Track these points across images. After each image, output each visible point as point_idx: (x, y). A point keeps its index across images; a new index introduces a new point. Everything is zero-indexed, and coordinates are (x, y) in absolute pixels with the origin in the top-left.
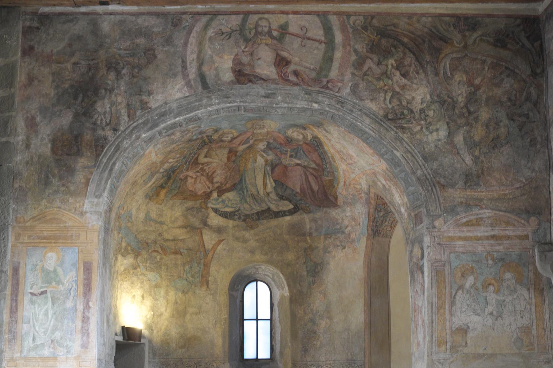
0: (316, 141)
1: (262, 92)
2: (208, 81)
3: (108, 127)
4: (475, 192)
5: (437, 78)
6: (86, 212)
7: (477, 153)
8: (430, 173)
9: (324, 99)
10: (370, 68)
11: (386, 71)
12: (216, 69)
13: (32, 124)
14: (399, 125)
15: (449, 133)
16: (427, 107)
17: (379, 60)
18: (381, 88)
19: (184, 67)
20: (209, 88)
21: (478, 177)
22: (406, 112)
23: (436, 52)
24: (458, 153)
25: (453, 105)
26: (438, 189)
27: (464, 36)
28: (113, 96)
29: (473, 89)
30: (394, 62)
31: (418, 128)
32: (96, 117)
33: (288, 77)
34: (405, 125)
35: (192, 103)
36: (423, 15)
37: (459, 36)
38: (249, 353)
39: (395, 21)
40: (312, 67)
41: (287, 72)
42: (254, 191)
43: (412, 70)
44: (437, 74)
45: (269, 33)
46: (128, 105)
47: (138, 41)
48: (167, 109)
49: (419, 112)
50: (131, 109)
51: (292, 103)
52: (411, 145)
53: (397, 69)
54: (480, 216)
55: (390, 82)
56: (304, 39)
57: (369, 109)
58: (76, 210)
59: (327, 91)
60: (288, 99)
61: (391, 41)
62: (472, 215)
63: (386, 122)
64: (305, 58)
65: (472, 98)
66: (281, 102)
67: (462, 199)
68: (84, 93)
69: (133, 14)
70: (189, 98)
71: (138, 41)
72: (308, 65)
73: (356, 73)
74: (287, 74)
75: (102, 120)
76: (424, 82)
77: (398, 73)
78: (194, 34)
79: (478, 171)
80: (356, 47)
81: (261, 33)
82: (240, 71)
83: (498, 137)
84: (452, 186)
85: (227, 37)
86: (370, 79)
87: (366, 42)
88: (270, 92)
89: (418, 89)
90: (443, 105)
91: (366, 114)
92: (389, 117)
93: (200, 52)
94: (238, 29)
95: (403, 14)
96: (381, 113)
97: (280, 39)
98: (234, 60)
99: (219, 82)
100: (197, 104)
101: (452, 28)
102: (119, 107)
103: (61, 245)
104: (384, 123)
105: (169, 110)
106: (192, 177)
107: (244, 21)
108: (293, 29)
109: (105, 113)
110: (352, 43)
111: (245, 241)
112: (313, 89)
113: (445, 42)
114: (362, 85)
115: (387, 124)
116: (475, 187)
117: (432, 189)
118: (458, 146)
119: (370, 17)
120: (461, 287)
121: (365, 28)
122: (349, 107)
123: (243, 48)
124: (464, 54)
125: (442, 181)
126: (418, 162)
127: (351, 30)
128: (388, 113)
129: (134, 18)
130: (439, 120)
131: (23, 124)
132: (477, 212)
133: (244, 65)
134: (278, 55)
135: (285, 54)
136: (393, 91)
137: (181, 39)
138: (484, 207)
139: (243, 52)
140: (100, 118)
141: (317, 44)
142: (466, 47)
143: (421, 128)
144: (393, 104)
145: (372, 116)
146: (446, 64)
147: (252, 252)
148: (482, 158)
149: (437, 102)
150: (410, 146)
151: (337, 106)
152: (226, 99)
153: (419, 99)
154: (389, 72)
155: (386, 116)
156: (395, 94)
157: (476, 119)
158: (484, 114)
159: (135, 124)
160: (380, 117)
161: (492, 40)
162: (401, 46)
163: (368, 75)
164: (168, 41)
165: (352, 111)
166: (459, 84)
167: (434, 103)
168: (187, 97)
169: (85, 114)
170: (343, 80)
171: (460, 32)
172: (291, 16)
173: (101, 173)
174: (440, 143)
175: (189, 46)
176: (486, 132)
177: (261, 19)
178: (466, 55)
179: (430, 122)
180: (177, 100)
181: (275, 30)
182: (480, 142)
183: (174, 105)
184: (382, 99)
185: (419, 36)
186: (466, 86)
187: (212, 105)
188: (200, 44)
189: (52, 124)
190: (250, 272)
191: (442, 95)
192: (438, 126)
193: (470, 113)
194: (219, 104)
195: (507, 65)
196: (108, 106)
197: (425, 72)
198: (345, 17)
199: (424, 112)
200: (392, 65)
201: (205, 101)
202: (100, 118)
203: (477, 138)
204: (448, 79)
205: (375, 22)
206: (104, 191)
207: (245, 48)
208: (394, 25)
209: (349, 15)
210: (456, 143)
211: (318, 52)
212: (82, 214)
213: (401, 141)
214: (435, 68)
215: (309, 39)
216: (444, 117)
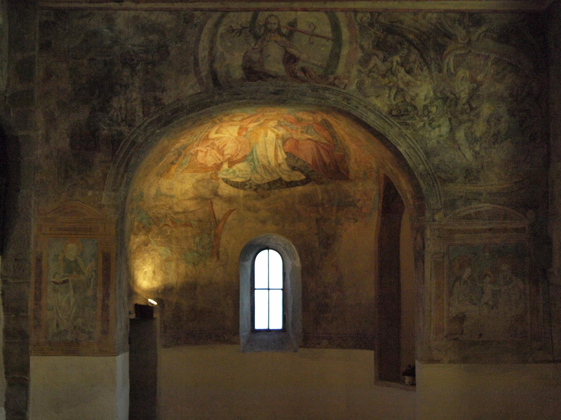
1: (271, 89)
2: (219, 78)
3: (124, 123)
4: (475, 186)
5: (441, 75)
6: (104, 206)
7: (477, 149)
8: (432, 168)
9: (331, 96)
10: (376, 65)
11: (391, 68)
12: (228, 65)
13: (51, 120)
14: (402, 121)
15: (451, 129)
16: (430, 103)
17: (385, 57)
18: (386, 85)
19: (196, 64)
20: (220, 85)
21: (478, 172)
22: (409, 108)
23: (441, 49)
24: (459, 148)
26: (439, 184)
27: (468, 32)
28: (128, 91)
29: (475, 86)
30: (399, 59)
31: (422, 124)
34: (408, 122)
36: (430, 11)
37: (464, 32)
38: (260, 324)
39: (402, 17)
40: (319, 64)
43: (416, 66)
44: (440, 71)
45: (279, 30)
46: (143, 101)
47: (151, 37)
48: (180, 105)
49: (422, 108)
52: (414, 141)
53: (402, 65)
54: (479, 210)
55: (395, 79)
56: (312, 35)
57: (374, 105)
58: (94, 203)
59: (334, 88)
61: (396, 37)
62: (471, 208)
63: (391, 119)
64: (313, 55)
65: (473, 95)
67: (462, 194)
68: (99, 88)
69: (146, 10)
71: (151, 37)
72: (315, 62)
73: (362, 70)
74: (295, 71)
75: (117, 116)
76: (428, 79)
77: (402, 70)
78: (206, 31)
79: (478, 166)
80: (363, 43)
81: (270, 31)
82: (250, 68)
83: (499, 132)
84: (452, 181)
85: (238, 34)
86: (375, 75)
87: (373, 38)
88: (278, 88)
89: (422, 86)
90: (445, 101)
91: (370, 110)
92: (393, 114)
93: (211, 49)
94: (248, 26)
95: (409, 10)
96: (386, 109)
97: (290, 36)
98: (244, 57)
99: (230, 79)
100: (209, 100)
101: (457, 25)
103: (80, 236)
104: (388, 119)
107: (255, 18)
108: (301, 26)
110: (359, 41)
111: (257, 211)
112: (320, 85)
113: (450, 39)
114: (368, 81)
115: (391, 121)
116: (475, 181)
117: (433, 183)
118: (459, 142)
119: (377, 14)
120: (458, 278)
121: (371, 25)
123: (253, 45)
124: (468, 51)
125: (443, 176)
126: (420, 157)
127: (357, 27)
128: (392, 110)
129: (145, 14)
130: (442, 117)
132: (476, 206)
134: (286, 52)
135: (293, 51)
136: (398, 87)
137: (193, 36)
138: (483, 200)
139: (254, 49)
140: (115, 114)
141: (324, 41)
142: (470, 42)
143: (424, 124)
144: (398, 101)
145: (377, 112)
146: (450, 60)
147: (264, 222)
148: (482, 153)
149: (440, 98)
150: (413, 142)
152: (236, 96)
153: (422, 96)
154: (394, 69)
155: (390, 113)
156: (400, 91)
157: (478, 115)
158: (486, 110)
159: (149, 120)
160: (384, 113)
161: (495, 36)
162: (406, 43)
163: (374, 72)
164: (181, 37)
165: (357, 107)
166: (462, 80)
168: (200, 93)
171: (464, 28)
172: (299, 13)
173: (118, 167)
174: (442, 138)
175: (201, 43)
176: (488, 128)
177: (270, 16)
178: (470, 51)
179: (433, 118)
180: (189, 97)
181: (284, 27)
182: (481, 138)
184: (387, 95)
185: (424, 33)
186: (469, 83)
188: (212, 42)
190: (261, 241)
191: (444, 91)
192: (440, 122)
193: (472, 109)
195: (509, 61)
196: (124, 102)
197: (429, 68)
198: (352, 14)
200: (397, 62)
201: (216, 97)
203: (478, 134)
204: (452, 75)
205: (382, 19)
206: (120, 185)
207: (255, 45)
208: (401, 22)
209: (356, 11)
210: (457, 139)
211: (326, 48)
212: (101, 207)
213: (404, 136)
214: (439, 65)
215: (317, 36)
216: (447, 113)
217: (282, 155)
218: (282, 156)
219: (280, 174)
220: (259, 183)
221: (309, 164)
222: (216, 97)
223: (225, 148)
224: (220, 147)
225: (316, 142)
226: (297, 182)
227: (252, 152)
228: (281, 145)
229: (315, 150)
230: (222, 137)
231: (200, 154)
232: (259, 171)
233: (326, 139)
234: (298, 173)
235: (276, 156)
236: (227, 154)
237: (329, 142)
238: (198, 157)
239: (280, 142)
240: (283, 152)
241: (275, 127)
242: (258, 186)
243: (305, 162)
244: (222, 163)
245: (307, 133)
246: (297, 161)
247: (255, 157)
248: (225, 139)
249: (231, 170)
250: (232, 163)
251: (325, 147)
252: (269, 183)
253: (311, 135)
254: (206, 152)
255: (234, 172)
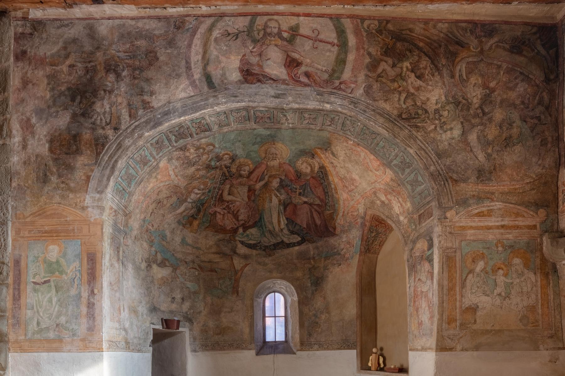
0: (322, 172)
9: (337, 100)
25: (468, 106)
32: (95, 117)
33: (299, 78)
35: (198, 102)
41: (298, 73)
42: (270, 227)
46: (129, 105)
48: (171, 108)
50: (132, 108)
51: (303, 103)
60: (298, 100)
66: (292, 103)
70: (194, 98)
90: (458, 106)
100: (203, 103)
102: (119, 108)
105: (173, 109)
106: (220, 213)
109: (104, 113)
122: (363, 108)
131: (18, 126)
133: (252, 65)
144: (408, 104)
149: (452, 103)
151: (350, 106)
152: (233, 98)
167: (448, 104)
169: (83, 115)
170: (356, 82)
183: (179, 105)
187: (219, 104)
189: (49, 125)
194: (226, 103)
199: (439, 113)
201: (211, 100)
202: (99, 118)
217: (284, 221)
218: (283, 221)
219: (282, 237)
220: (267, 244)
221: (304, 228)
222: (211, 100)
223: (239, 213)
224: (235, 212)
225: (311, 205)
226: (294, 243)
227: (261, 218)
228: (283, 211)
229: (309, 214)
230: (235, 201)
231: (219, 217)
232: (267, 235)
233: (319, 198)
234: (296, 236)
235: (279, 222)
236: (242, 220)
237: (322, 200)
238: (217, 218)
239: (282, 208)
240: (284, 218)
241: (278, 190)
242: (266, 247)
243: (301, 226)
244: (238, 228)
245: (303, 195)
246: (295, 226)
247: (263, 223)
248: (238, 203)
249: (245, 234)
250: (245, 228)
251: (317, 209)
252: (274, 245)
253: (307, 197)
254: (223, 215)
255: (247, 236)
